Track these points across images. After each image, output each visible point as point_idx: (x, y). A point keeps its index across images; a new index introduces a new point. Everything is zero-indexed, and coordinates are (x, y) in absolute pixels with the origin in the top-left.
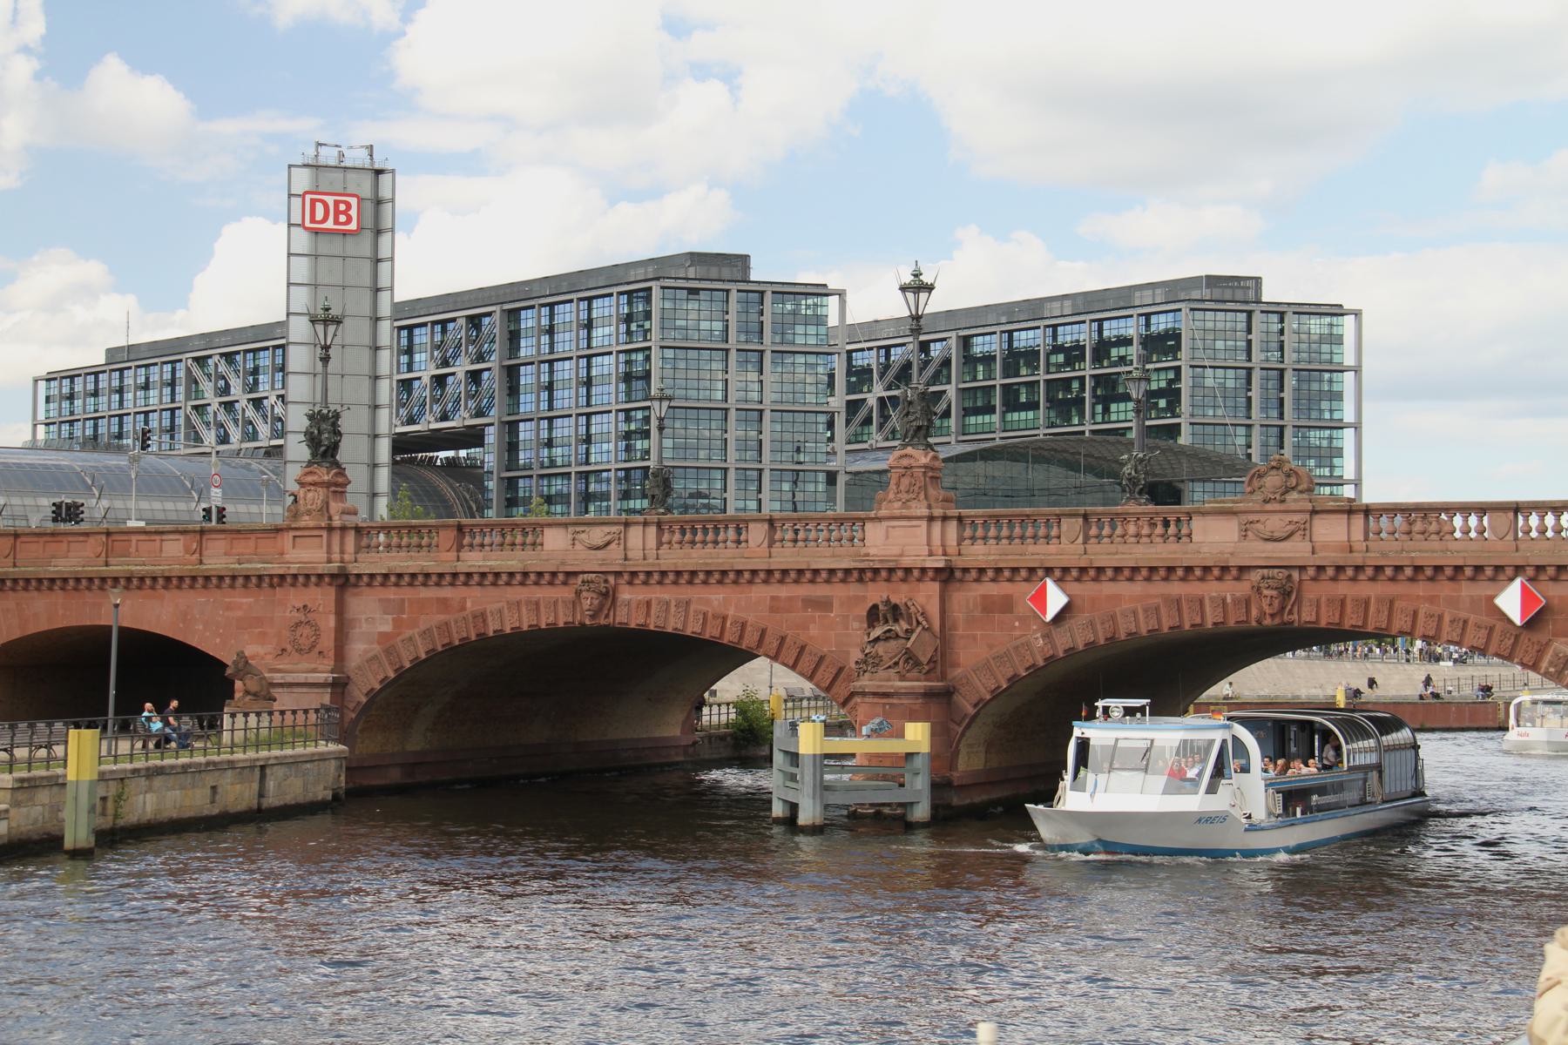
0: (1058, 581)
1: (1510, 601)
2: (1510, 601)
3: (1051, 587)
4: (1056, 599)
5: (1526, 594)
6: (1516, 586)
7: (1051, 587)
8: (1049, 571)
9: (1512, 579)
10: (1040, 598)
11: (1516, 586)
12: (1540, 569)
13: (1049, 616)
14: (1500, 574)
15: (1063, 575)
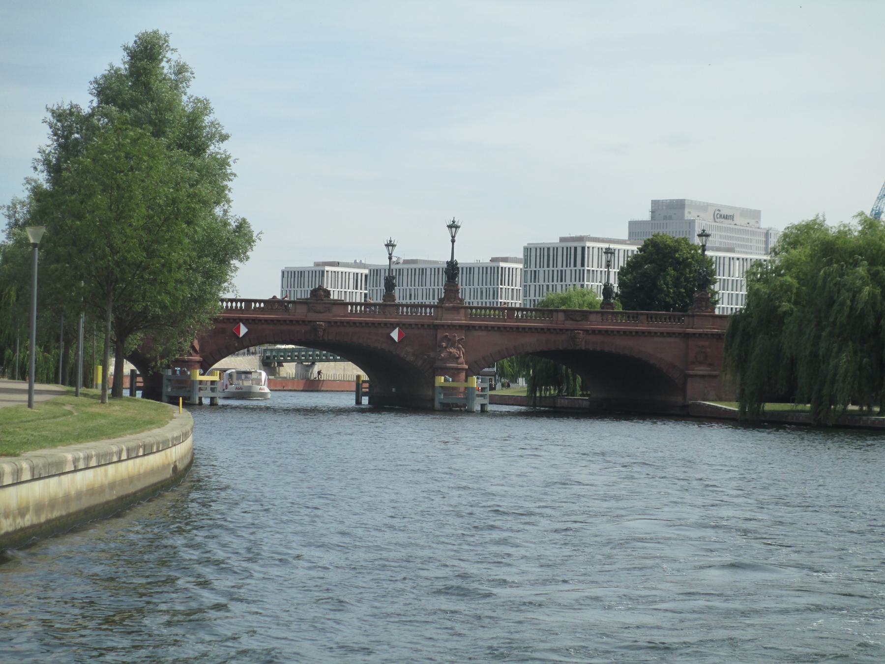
0: (243, 323)
1: (395, 335)
2: (395, 335)
3: (242, 326)
4: (243, 330)
5: (400, 334)
6: (397, 330)
7: (242, 326)
8: (241, 320)
9: (395, 328)
10: (239, 329)
11: (397, 330)
12: (404, 325)
13: (241, 335)
14: (393, 326)
15: (246, 322)
